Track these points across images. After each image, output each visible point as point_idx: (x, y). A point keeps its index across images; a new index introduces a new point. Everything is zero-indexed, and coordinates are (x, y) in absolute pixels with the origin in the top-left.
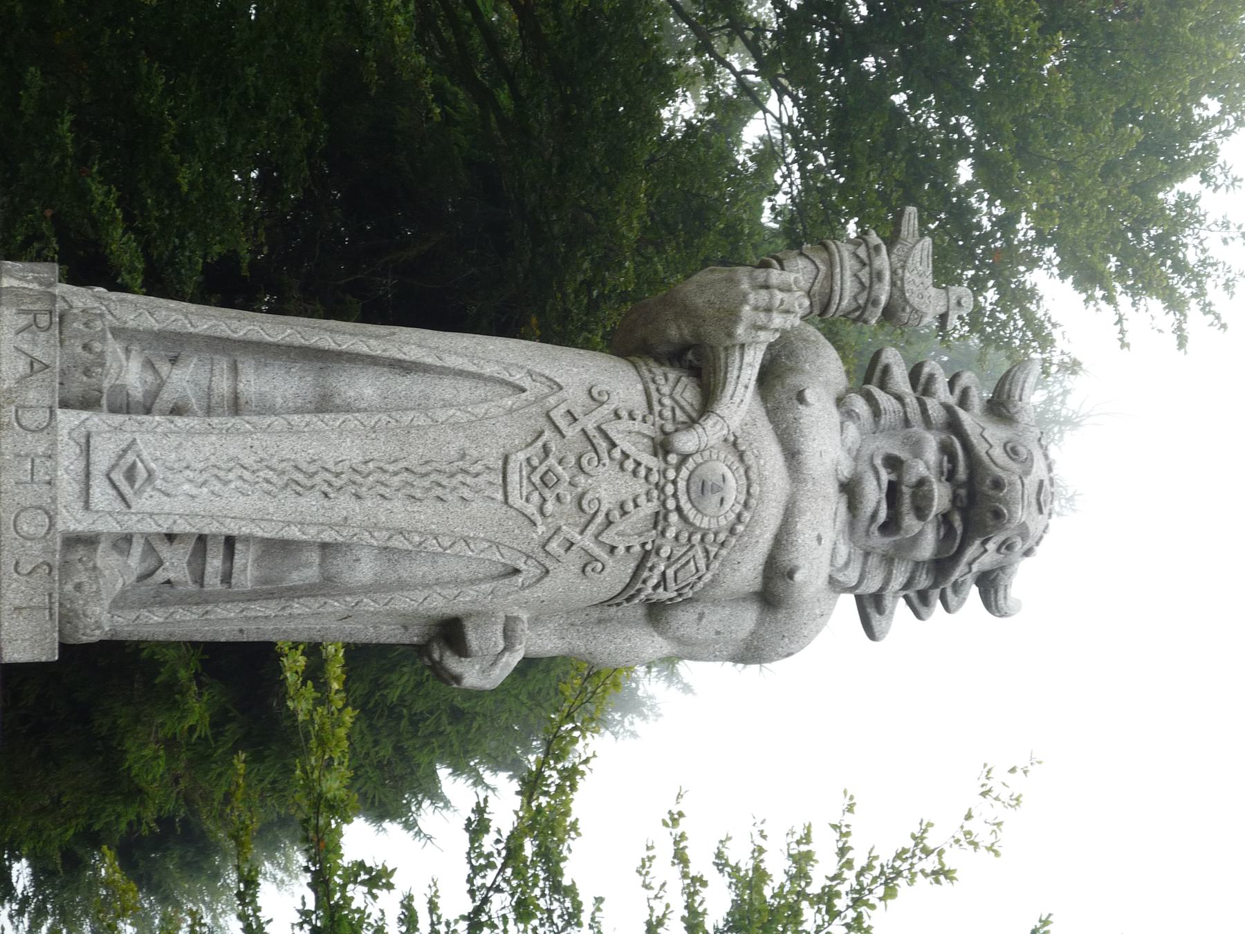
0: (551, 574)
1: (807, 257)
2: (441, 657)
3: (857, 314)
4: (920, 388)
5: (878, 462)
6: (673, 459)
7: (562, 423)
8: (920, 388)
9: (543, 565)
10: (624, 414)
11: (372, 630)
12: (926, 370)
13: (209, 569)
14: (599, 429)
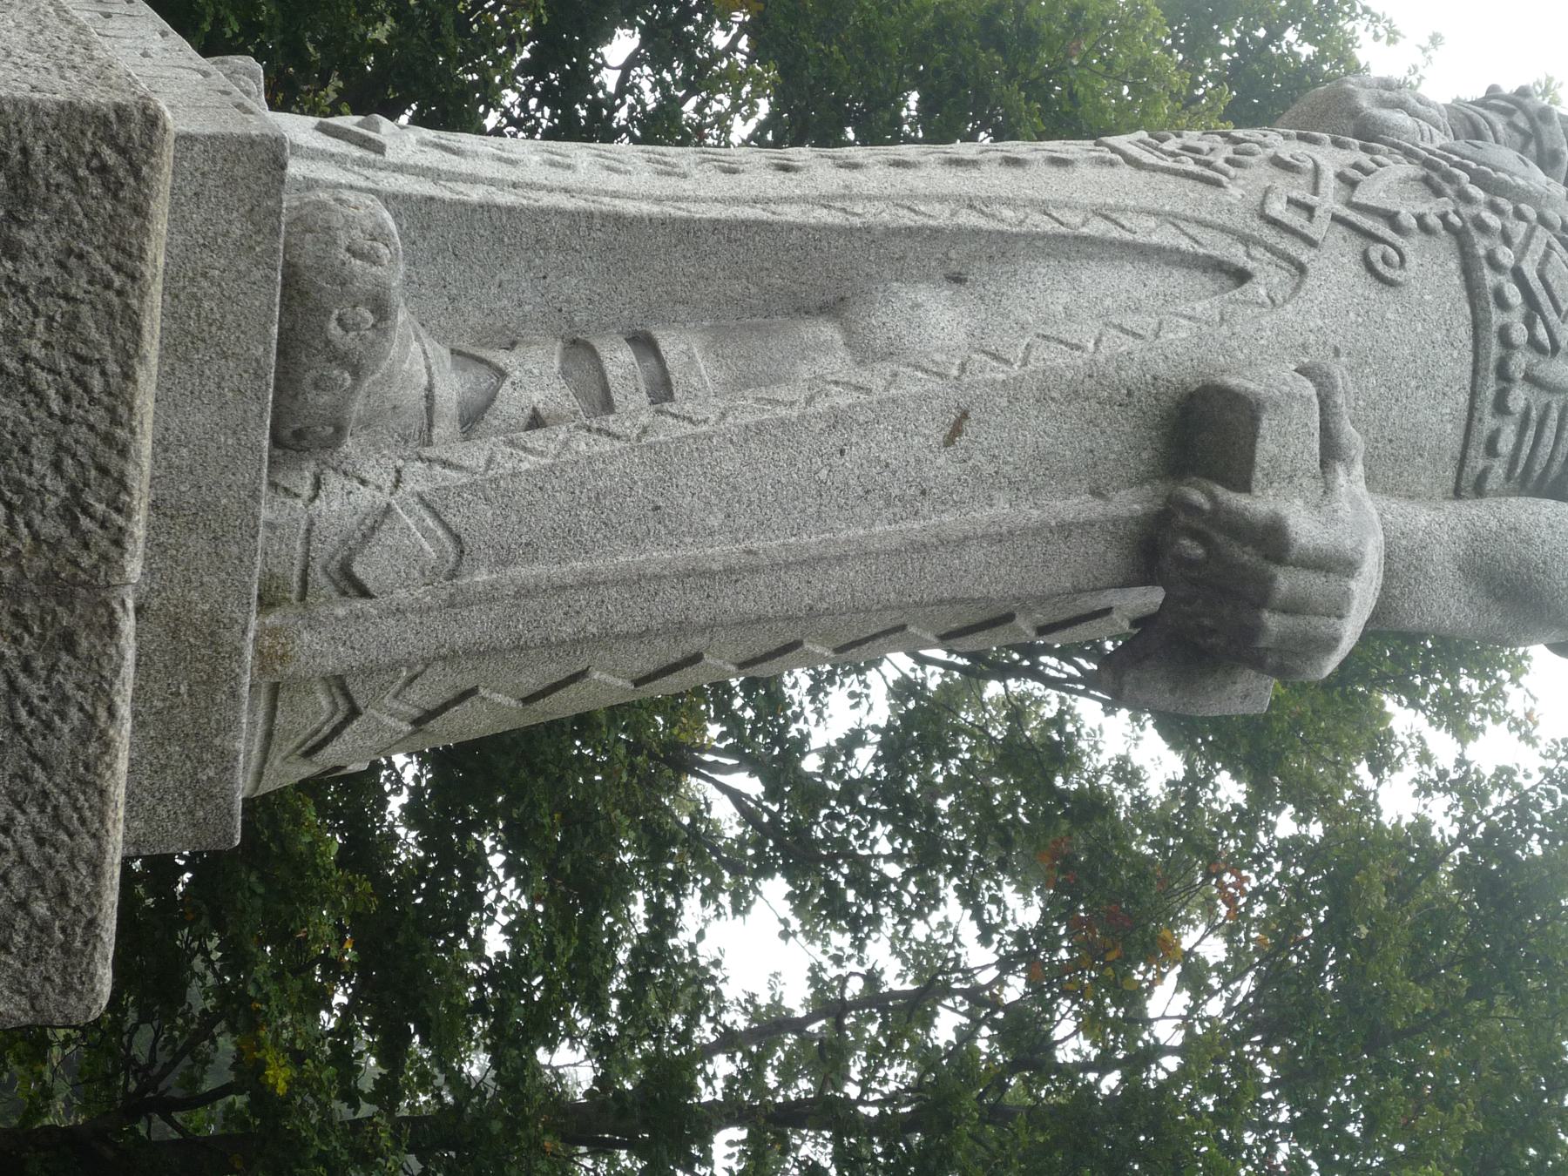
0: (1311, 271)
2: (1212, 497)
9: (1291, 260)
11: (1035, 513)
13: (614, 371)
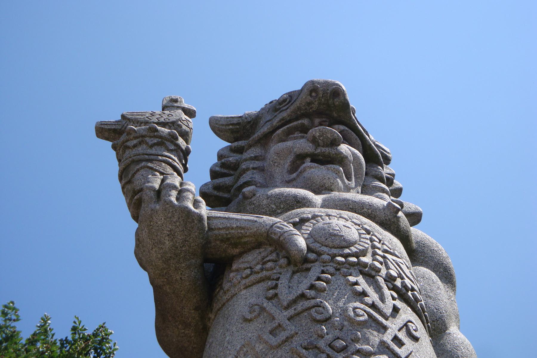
1: (133, 175)
3: (181, 154)
4: (232, 172)
5: (294, 175)
6: (312, 256)
7: (283, 336)
8: (232, 172)
10: (272, 292)
12: (217, 169)
14: (287, 308)
